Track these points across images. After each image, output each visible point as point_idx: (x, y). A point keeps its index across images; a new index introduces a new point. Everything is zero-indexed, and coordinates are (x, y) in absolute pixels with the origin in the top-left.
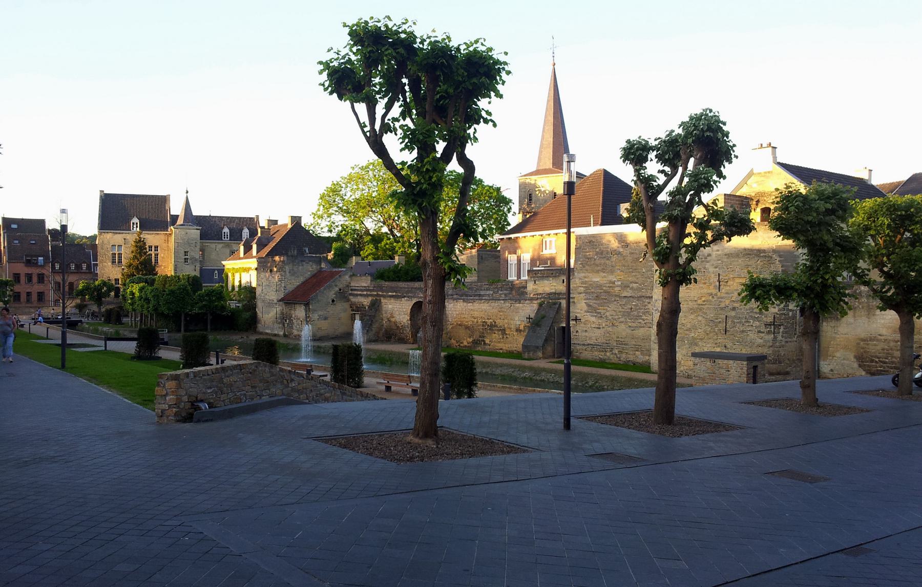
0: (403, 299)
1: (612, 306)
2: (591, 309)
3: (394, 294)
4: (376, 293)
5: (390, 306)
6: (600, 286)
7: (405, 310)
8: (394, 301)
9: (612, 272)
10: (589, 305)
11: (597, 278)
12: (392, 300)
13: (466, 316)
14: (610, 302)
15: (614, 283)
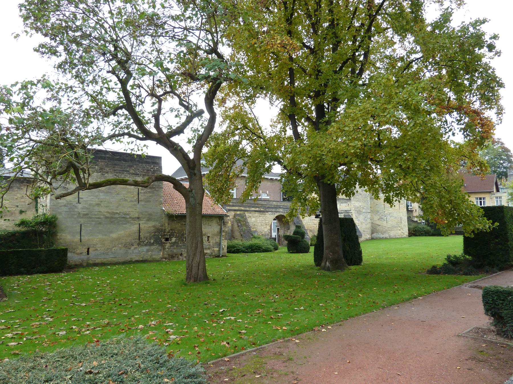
0: (267, 213)
1: (361, 216)
2: (357, 218)
3: (257, 209)
4: (237, 208)
5: (253, 219)
6: (358, 208)
7: (267, 222)
8: (259, 215)
9: (360, 201)
10: (356, 216)
11: (357, 204)
12: (257, 214)
13: (311, 224)
14: (361, 214)
15: (360, 206)
